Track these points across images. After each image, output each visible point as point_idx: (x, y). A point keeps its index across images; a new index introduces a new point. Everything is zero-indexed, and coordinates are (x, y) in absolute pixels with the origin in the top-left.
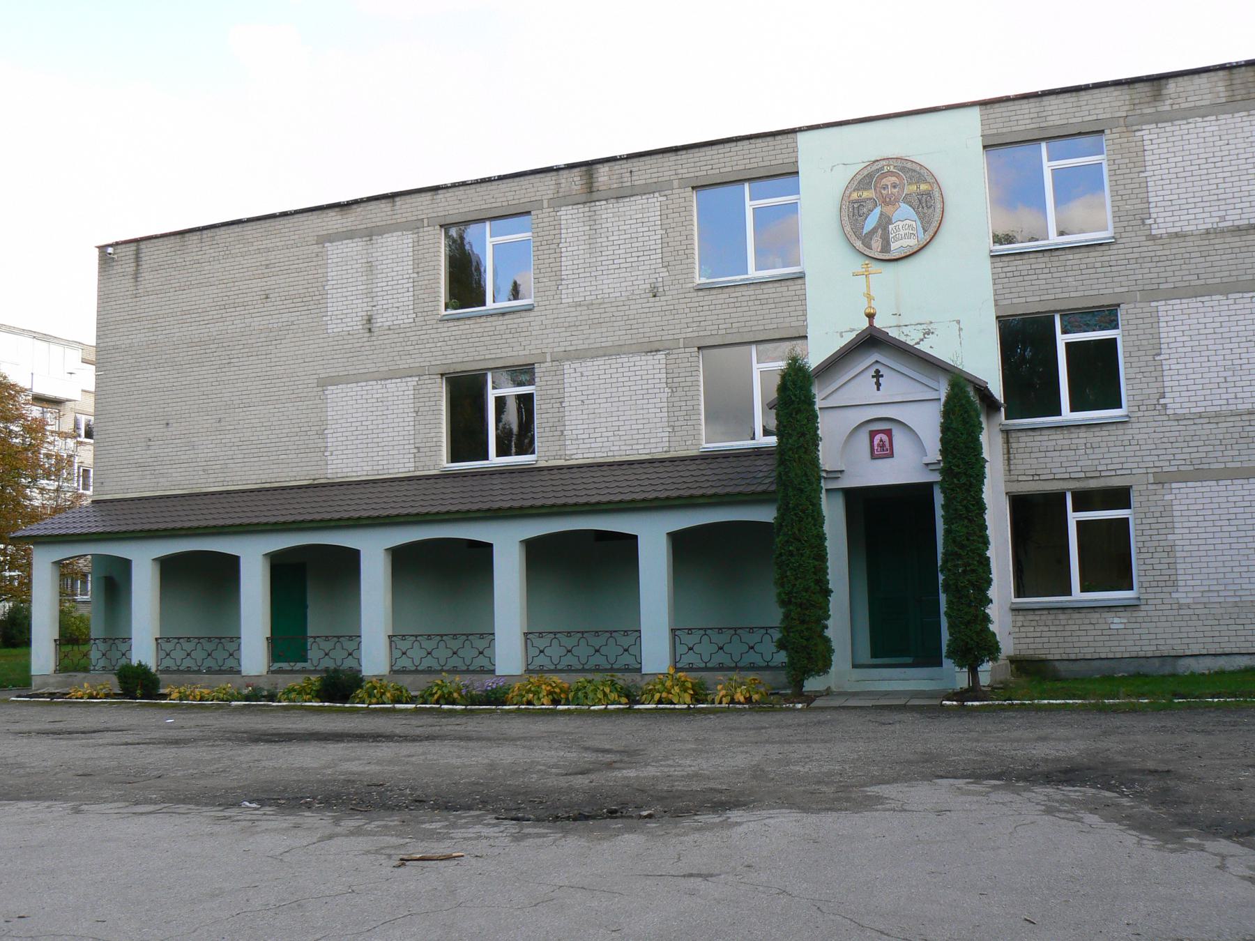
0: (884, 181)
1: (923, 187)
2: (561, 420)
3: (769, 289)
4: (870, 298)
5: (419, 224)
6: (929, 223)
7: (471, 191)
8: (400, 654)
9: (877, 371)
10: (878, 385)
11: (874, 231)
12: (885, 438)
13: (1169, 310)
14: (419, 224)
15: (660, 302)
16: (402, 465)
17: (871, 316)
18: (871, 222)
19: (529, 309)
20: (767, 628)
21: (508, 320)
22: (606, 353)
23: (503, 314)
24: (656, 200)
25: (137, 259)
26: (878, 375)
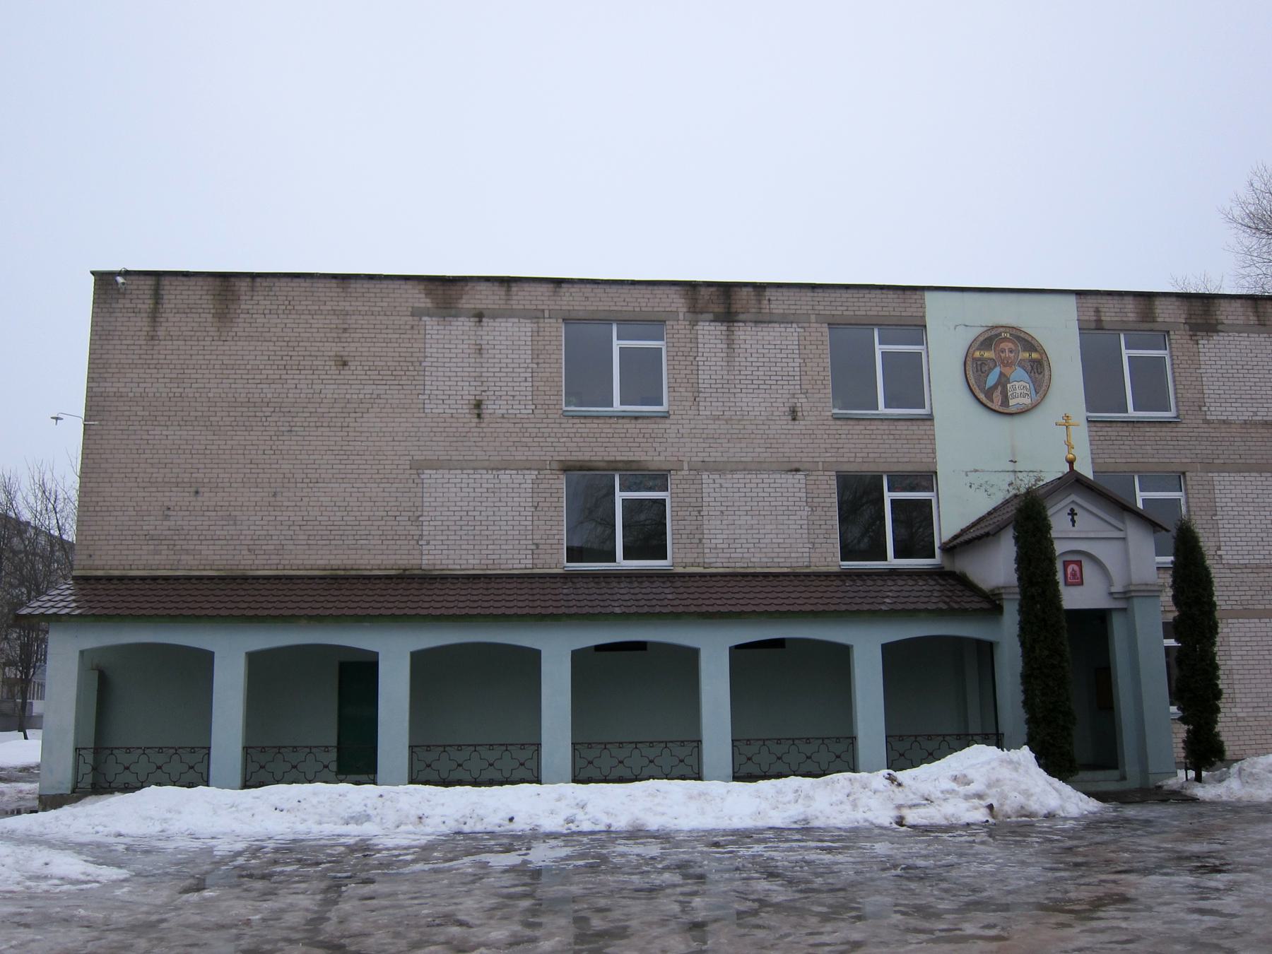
0: (1002, 345)
1: (1034, 355)
2: (700, 528)
3: (902, 426)
4: (1070, 446)
5: (539, 314)
6: (1040, 386)
7: (599, 290)
8: (528, 764)
9: (1072, 510)
10: (1073, 521)
11: (995, 387)
12: (1076, 568)
13: (1222, 481)
14: (539, 314)
15: (800, 425)
16: (517, 560)
17: (1071, 463)
18: (992, 379)
19: (666, 416)
20: (944, 736)
21: (641, 424)
22: (746, 468)
23: (636, 418)
24: (793, 332)
25: (157, 297)
26: (1072, 513)
